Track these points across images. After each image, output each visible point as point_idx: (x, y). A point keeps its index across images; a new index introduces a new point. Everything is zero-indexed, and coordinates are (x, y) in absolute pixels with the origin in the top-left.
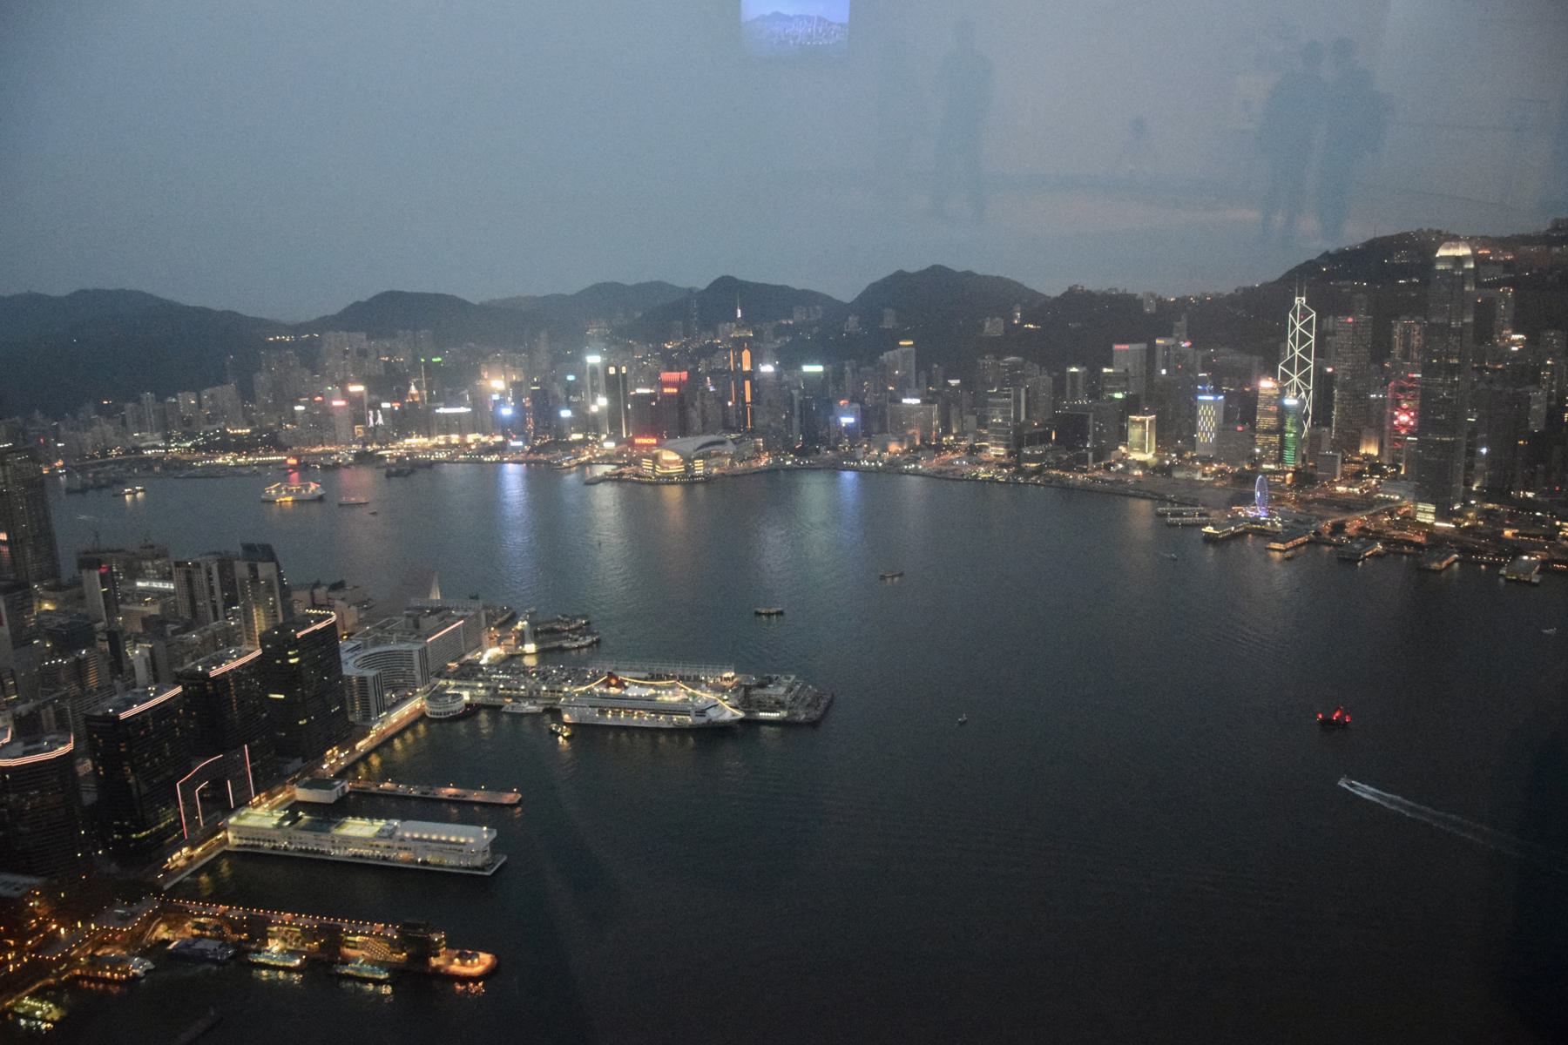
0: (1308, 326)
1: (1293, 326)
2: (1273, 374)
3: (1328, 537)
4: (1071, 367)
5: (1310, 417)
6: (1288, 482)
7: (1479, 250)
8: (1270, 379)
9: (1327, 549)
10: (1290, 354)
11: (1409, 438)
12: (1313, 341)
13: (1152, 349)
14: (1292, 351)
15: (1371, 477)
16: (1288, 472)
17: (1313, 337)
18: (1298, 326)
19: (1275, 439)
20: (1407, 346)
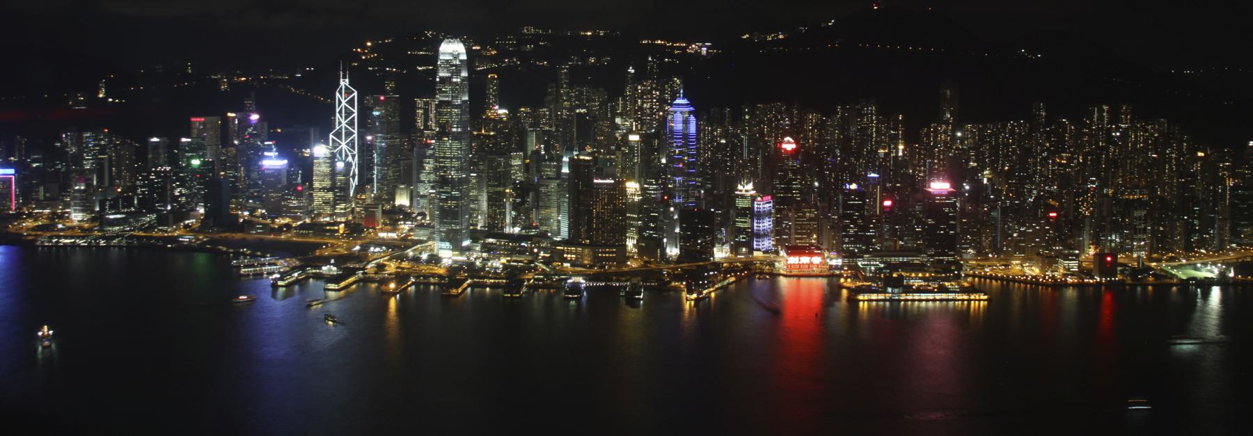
0: (351, 102)
1: (340, 103)
2: (327, 143)
3: (373, 275)
4: (152, 137)
5: (357, 177)
6: (341, 232)
7: (473, 46)
8: (323, 145)
9: (374, 286)
10: (339, 125)
11: (431, 191)
12: (355, 115)
13: (226, 120)
14: (340, 123)
15: (405, 224)
16: (341, 223)
17: (355, 111)
18: (344, 102)
19: (330, 195)
20: (427, 119)
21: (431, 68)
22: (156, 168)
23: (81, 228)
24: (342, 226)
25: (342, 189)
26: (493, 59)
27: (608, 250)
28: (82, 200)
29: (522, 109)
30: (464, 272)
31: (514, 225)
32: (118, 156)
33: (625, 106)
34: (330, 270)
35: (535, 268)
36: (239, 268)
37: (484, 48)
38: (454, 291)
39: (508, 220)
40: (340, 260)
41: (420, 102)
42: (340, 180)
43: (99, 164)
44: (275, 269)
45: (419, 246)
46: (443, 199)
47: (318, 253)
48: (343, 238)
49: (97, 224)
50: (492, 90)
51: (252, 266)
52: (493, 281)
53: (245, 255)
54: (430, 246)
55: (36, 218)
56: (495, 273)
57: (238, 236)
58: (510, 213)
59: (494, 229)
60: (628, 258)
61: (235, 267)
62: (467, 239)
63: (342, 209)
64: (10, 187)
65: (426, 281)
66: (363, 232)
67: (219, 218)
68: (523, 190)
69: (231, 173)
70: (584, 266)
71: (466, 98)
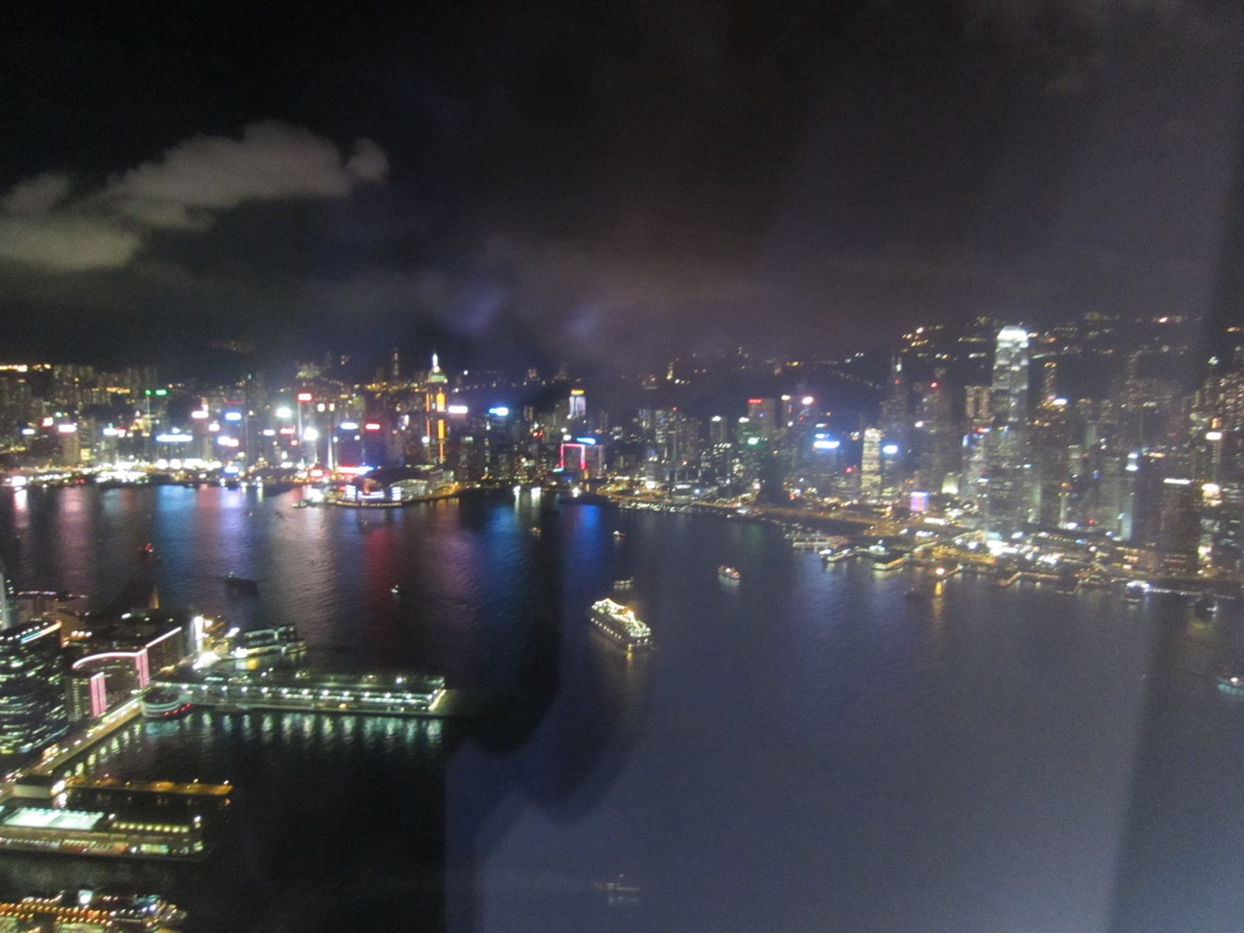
9: (919, 569)
16: (886, 506)
19: (878, 479)
20: (977, 408)
21: (983, 355)
22: (719, 444)
23: (654, 495)
24: (889, 509)
25: (890, 473)
26: (1050, 347)
27: (1176, 555)
28: (655, 470)
29: (1082, 400)
30: (1015, 563)
31: (1069, 520)
32: (685, 432)
33: (1203, 400)
34: (877, 550)
35: (1092, 568)
36: (791, 541)
37: (1041, 334)
38: (1003, 582)
39: (1062, 515)
40: (888, 542)
41: (971, 390)
42: (888, 465)
43: (669, 438)
44: (826, 548)
45: (966, 534)
46: (995, 490)
47: (865, 533)
48: (890, 520)
49: (667, 492)
50: (1049, 379)
51: (803, 540)
52: (1043, 576)
53: (797, 530)
54: (979, 534)
55: (618, 483)
56: (1049, 569)
57: (790, 512)
58: (1065, 508)
59: (1048, 521)
60: (1200, 567)
61: (787, 540)
62: (1017, 531)
63: (888, 493)
64: (597, 455)
65: (973, 569)
66: (908, 516)
67: (773, 494)
68: (1081, 486)
69: (784, 452)
70: (1147, 570)
71: (1025, 387)
